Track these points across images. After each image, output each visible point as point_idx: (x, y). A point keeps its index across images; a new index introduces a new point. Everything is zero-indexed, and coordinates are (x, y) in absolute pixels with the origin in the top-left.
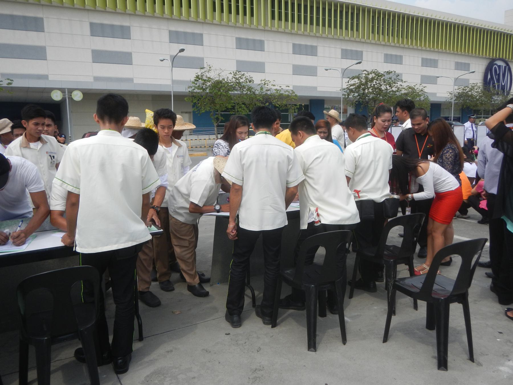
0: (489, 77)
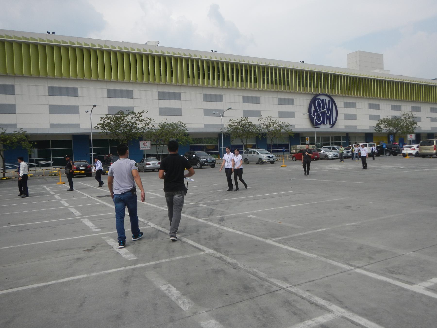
0: (313, 109)
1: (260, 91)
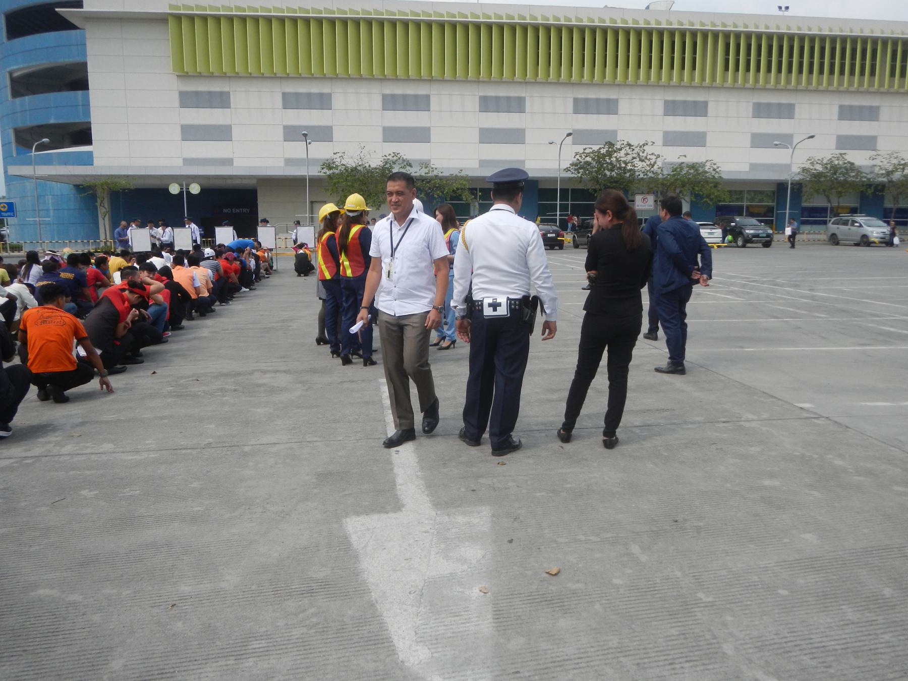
1: (882, 93)
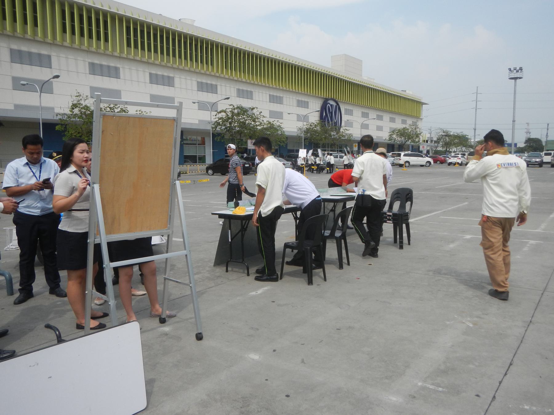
0: (324, 114)
